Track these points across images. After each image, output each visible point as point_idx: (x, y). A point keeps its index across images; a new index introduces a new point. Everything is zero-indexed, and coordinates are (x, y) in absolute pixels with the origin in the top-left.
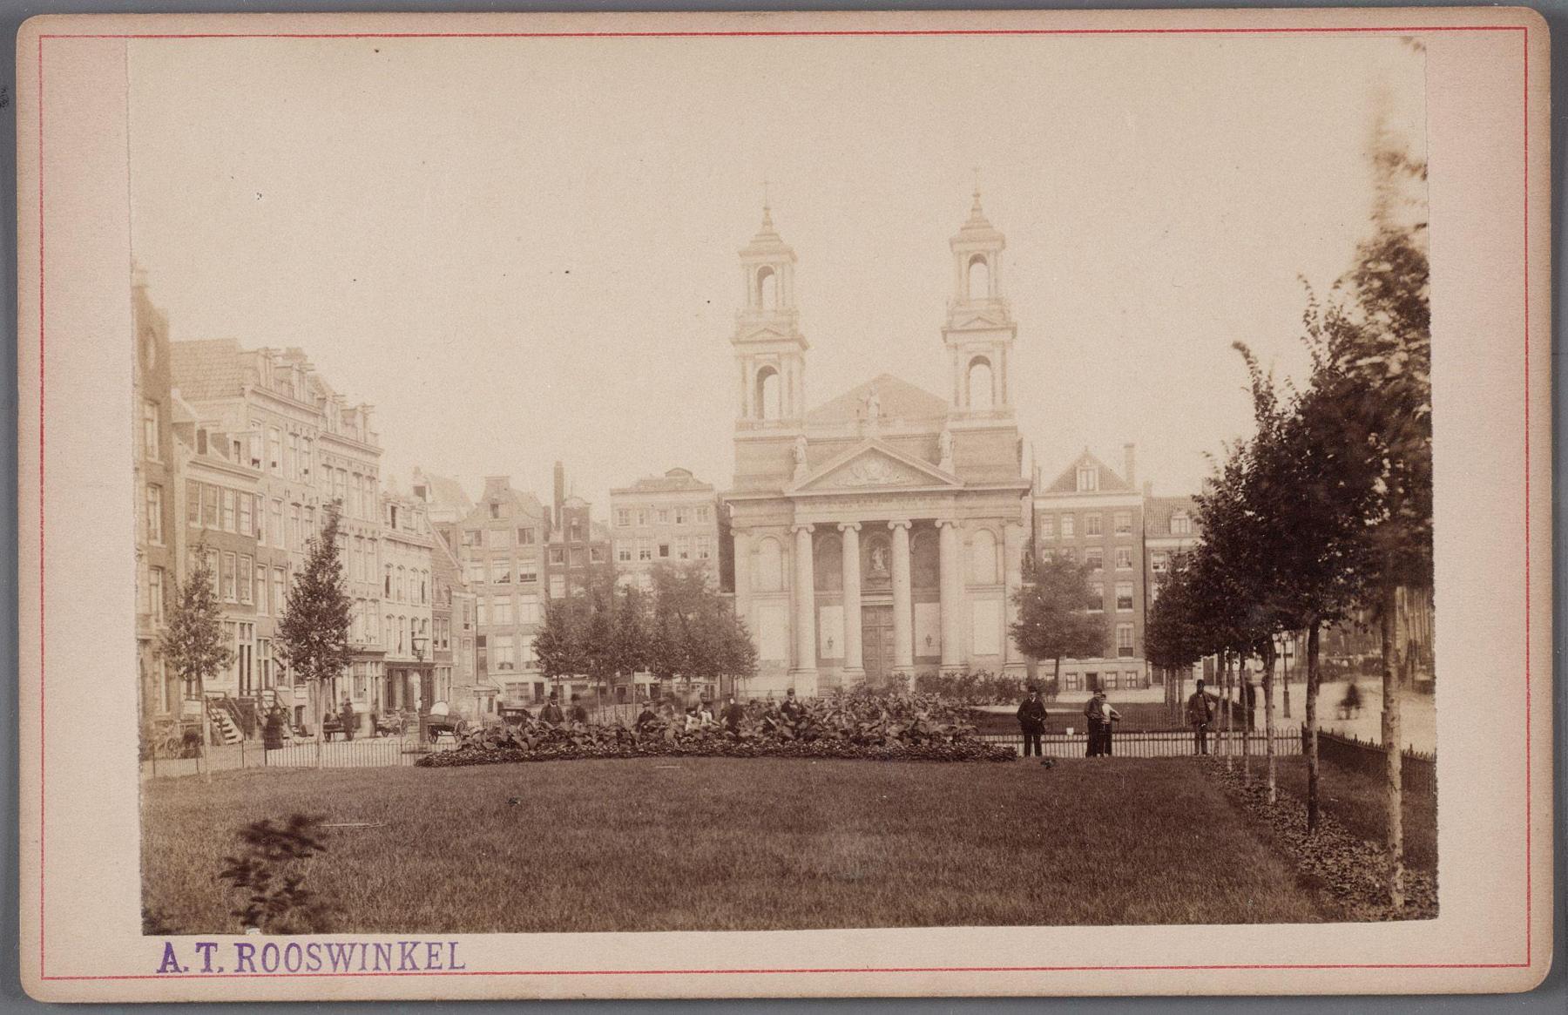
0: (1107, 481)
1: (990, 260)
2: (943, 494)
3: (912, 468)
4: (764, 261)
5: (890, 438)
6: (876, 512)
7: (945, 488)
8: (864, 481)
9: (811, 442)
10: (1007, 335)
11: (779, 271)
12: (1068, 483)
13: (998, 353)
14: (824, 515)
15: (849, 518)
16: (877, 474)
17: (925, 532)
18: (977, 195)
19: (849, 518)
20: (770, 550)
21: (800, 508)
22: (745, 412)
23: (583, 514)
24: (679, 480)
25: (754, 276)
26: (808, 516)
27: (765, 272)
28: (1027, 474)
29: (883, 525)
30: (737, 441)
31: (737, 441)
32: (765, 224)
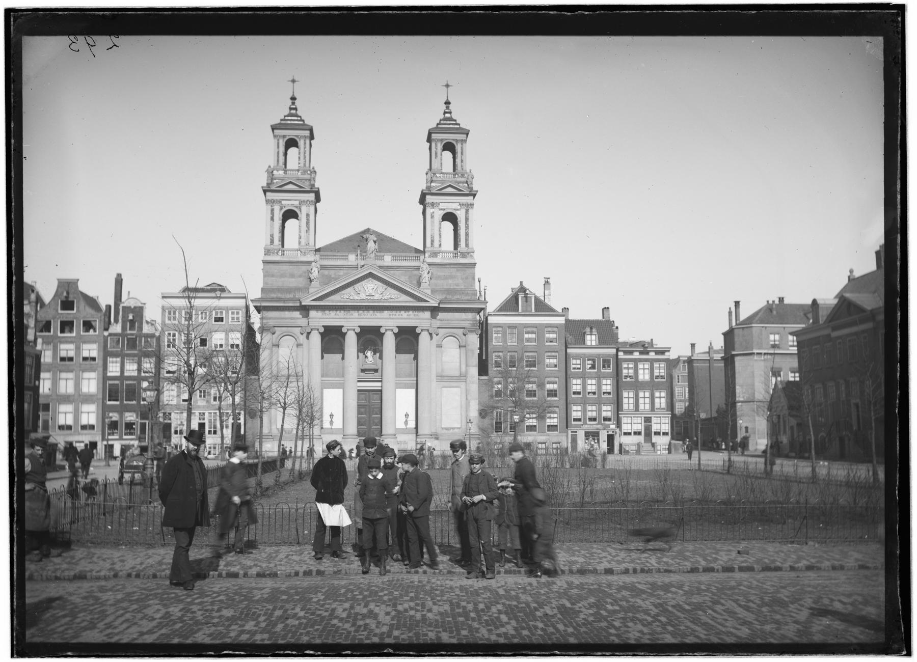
1: (458, 148)
5: (381, 267)
10: (469, 199)
12: (510, 306)
13: (463, 211)
15: (352, 322)
30: (264, 262)
31: (264, 262)
32: (291, 109)
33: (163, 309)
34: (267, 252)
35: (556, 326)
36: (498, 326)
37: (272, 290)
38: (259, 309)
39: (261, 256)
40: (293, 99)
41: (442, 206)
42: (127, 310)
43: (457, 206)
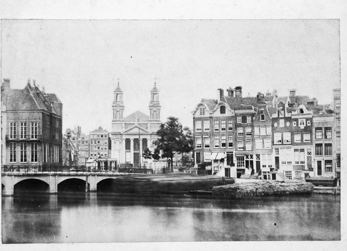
2: (147, 134)
3: (130, 129)
7: (148, 133)
8: (134, 131)
9: (125, 124)
14: (128, 137)
15: (132, 138)
16: (136, 131)
18: (155, 83)
19: (132, 138)
20: (118, 142)
21: (123, 136)
22: (114, 119)
26: (125, 137)
30: (112, 124)
31: (112, 124)
32: (118, 86)
34: (113, 121)
39: (111, 122)
40: (118, 83)
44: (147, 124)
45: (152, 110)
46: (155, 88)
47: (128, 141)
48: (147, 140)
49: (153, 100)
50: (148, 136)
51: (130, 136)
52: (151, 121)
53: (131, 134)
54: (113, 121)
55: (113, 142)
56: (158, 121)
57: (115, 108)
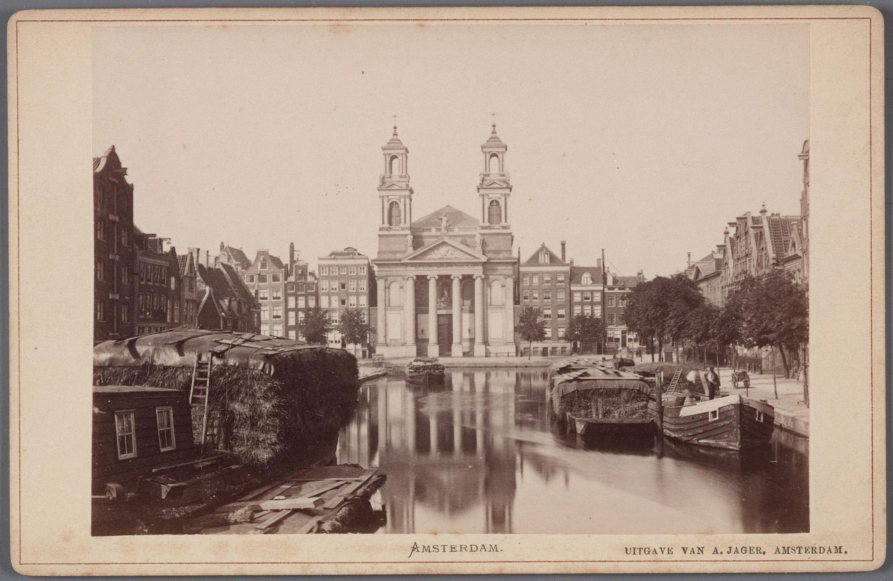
0: (553, 259)
1: (500, 156)
4: (394, 152)
5: (450, 237)
6: (444, 271)
10: (507, 191)
11: (400, 157)
12: (534, 260)
13: (503, 199)
14: (422, 271)
15: (432, 273)
17: (467, 281)
18: (494, 126)
19: (432, 273)
23: (304, 268)
24: (350, 252)
25: (388, 158)
26: (413, 272)
27: (394, 157)
28: (515, 255)
29: (448, 277)
30: (380, 236)
33: (319, 266)
34: (381, 229)
35: (564, 272)
36: (526, 274)
37: (385, 252)
38: (378, 265)
40: (395, 128)
41: (490, 196)
42: (298, 267)
43: (498, 196)
44: (474, 236)
45: (486, 199)
46: (494, 138)
47: (421, 283)
48: (474, 280)
49: (487, 173)
50: (476, 268)
51: (426, 268)
52: (483, 228)
53: (430, 265)
54: (381, 229)
55: (380, 284)
56: (504, 228)
57: (385, 193)
